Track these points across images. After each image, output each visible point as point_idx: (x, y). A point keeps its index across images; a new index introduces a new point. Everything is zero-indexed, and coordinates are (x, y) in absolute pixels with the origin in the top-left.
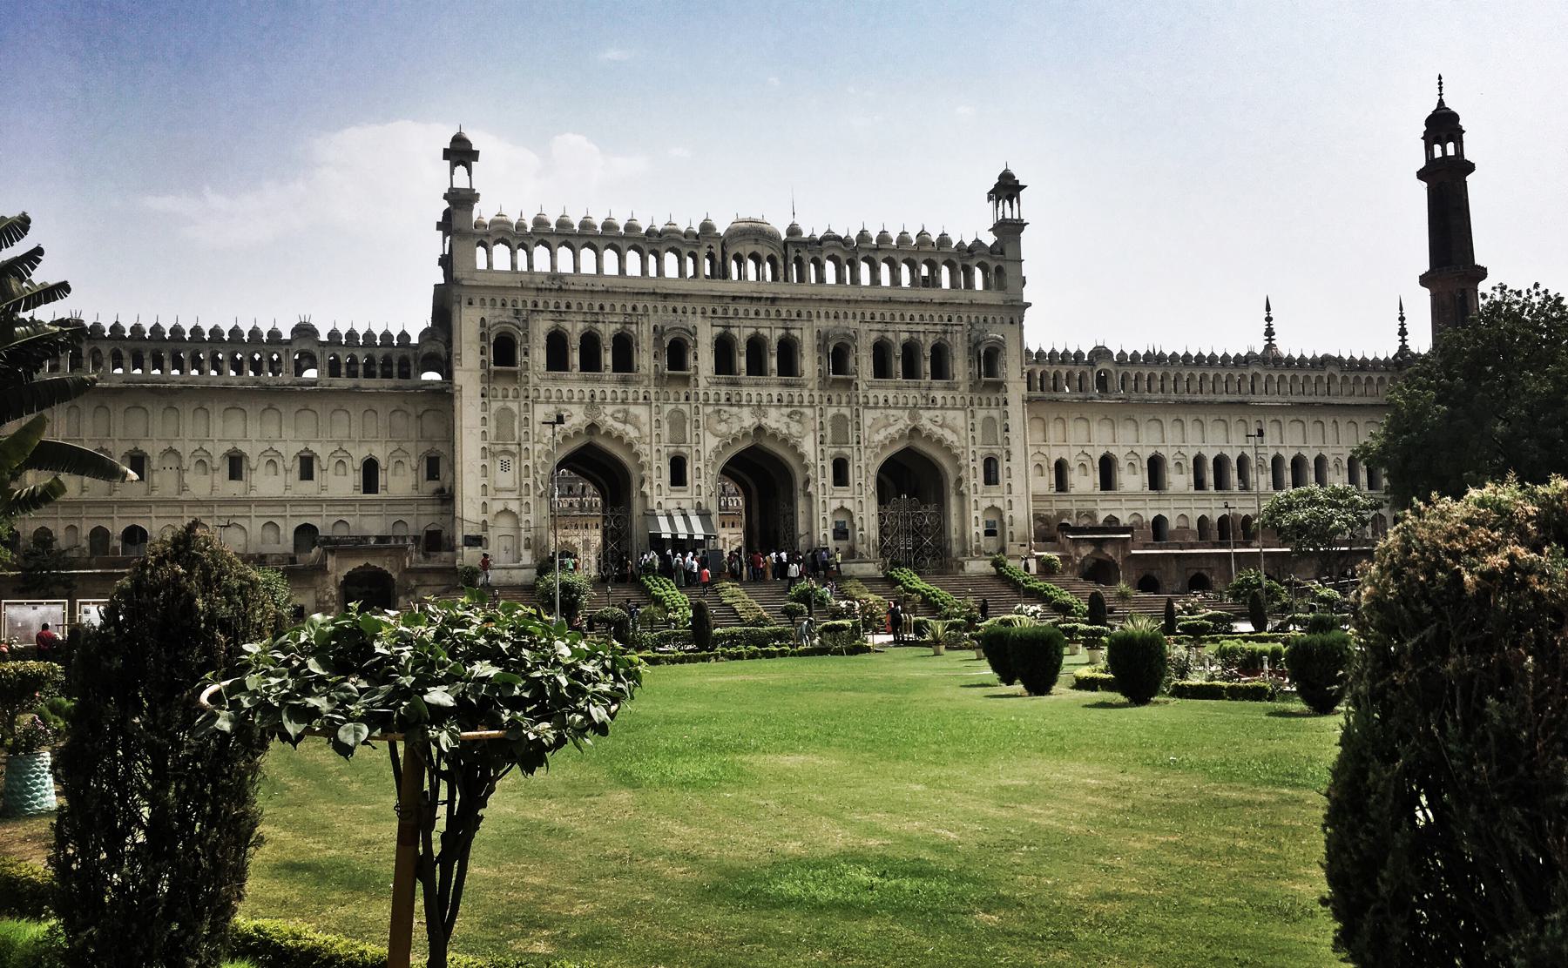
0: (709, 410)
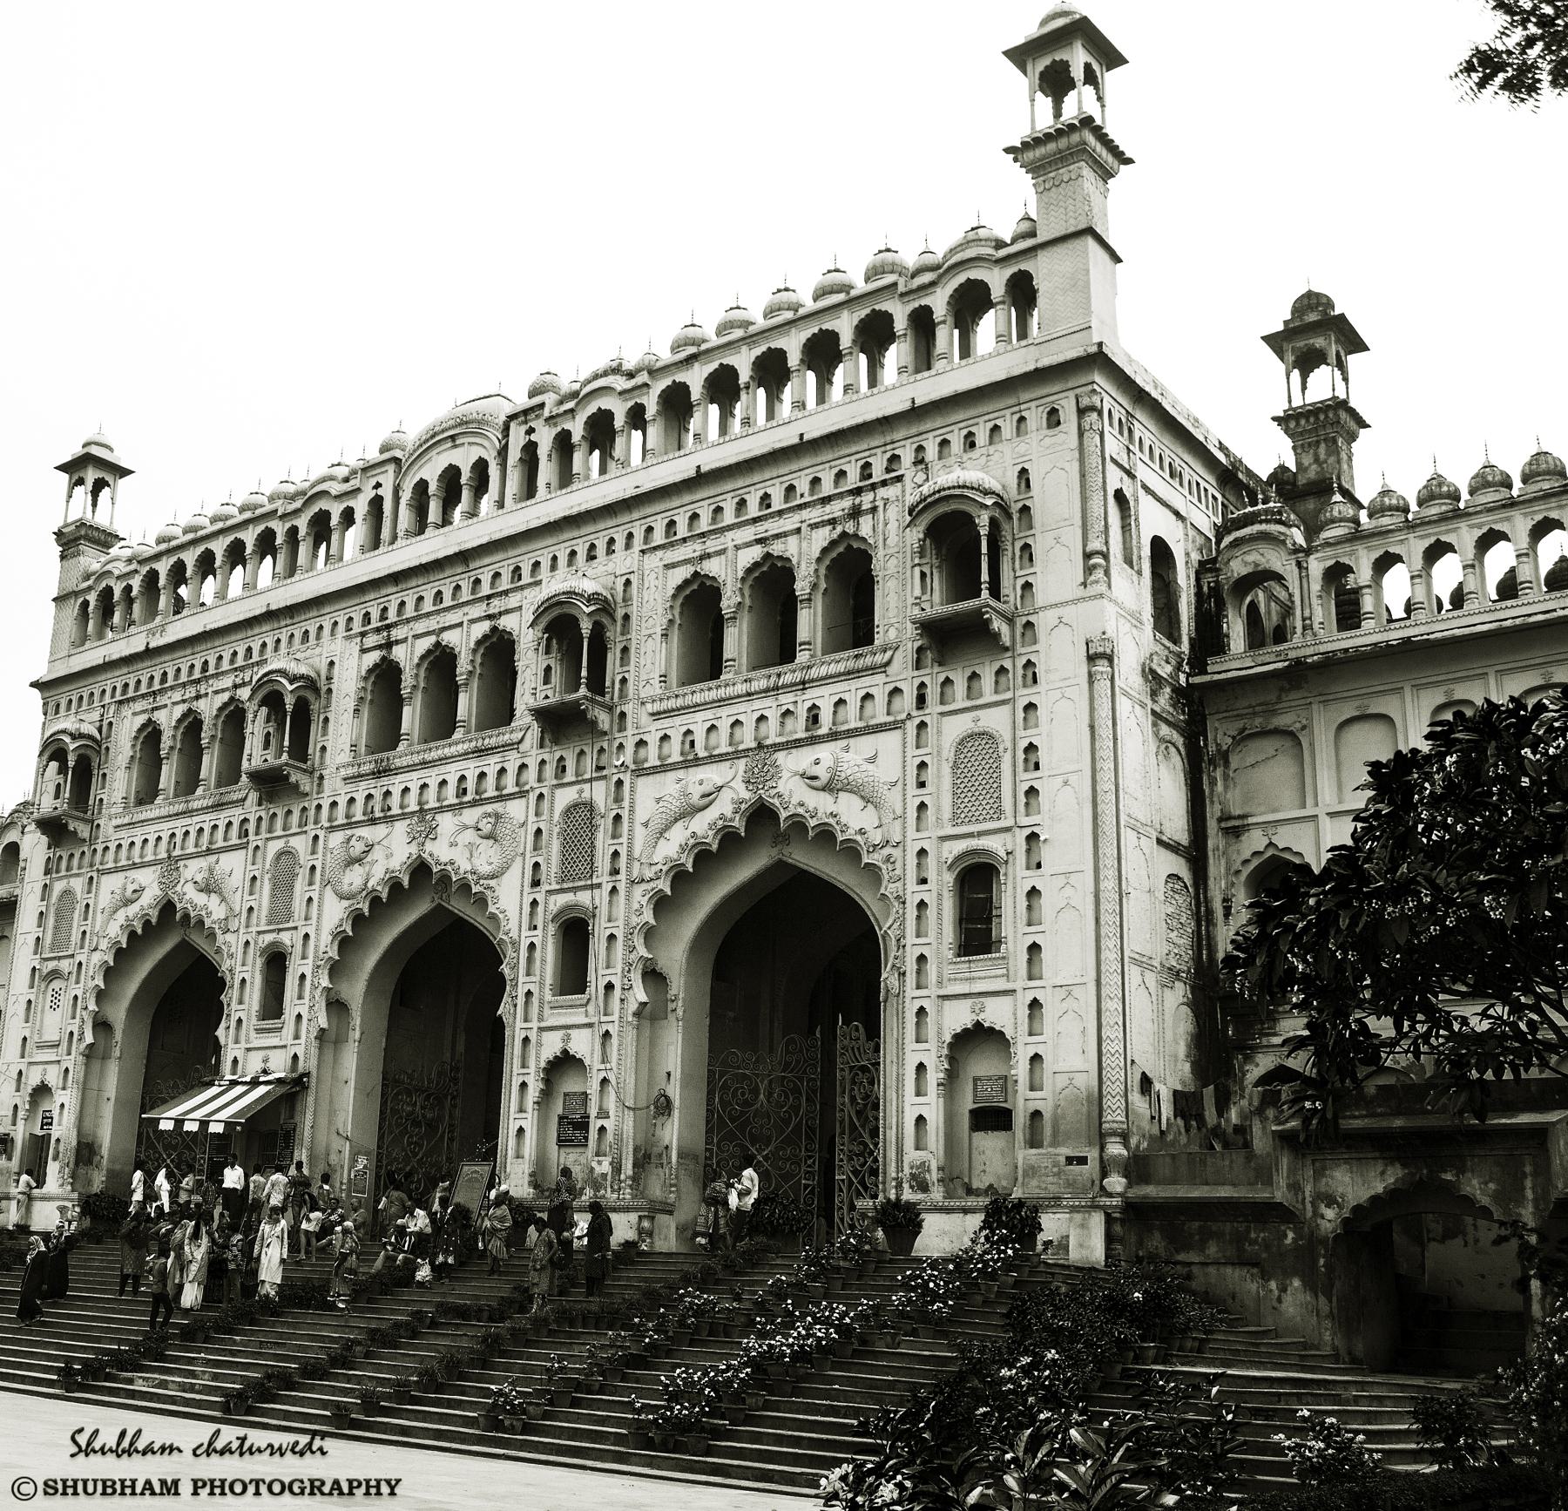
0: (337, 838)
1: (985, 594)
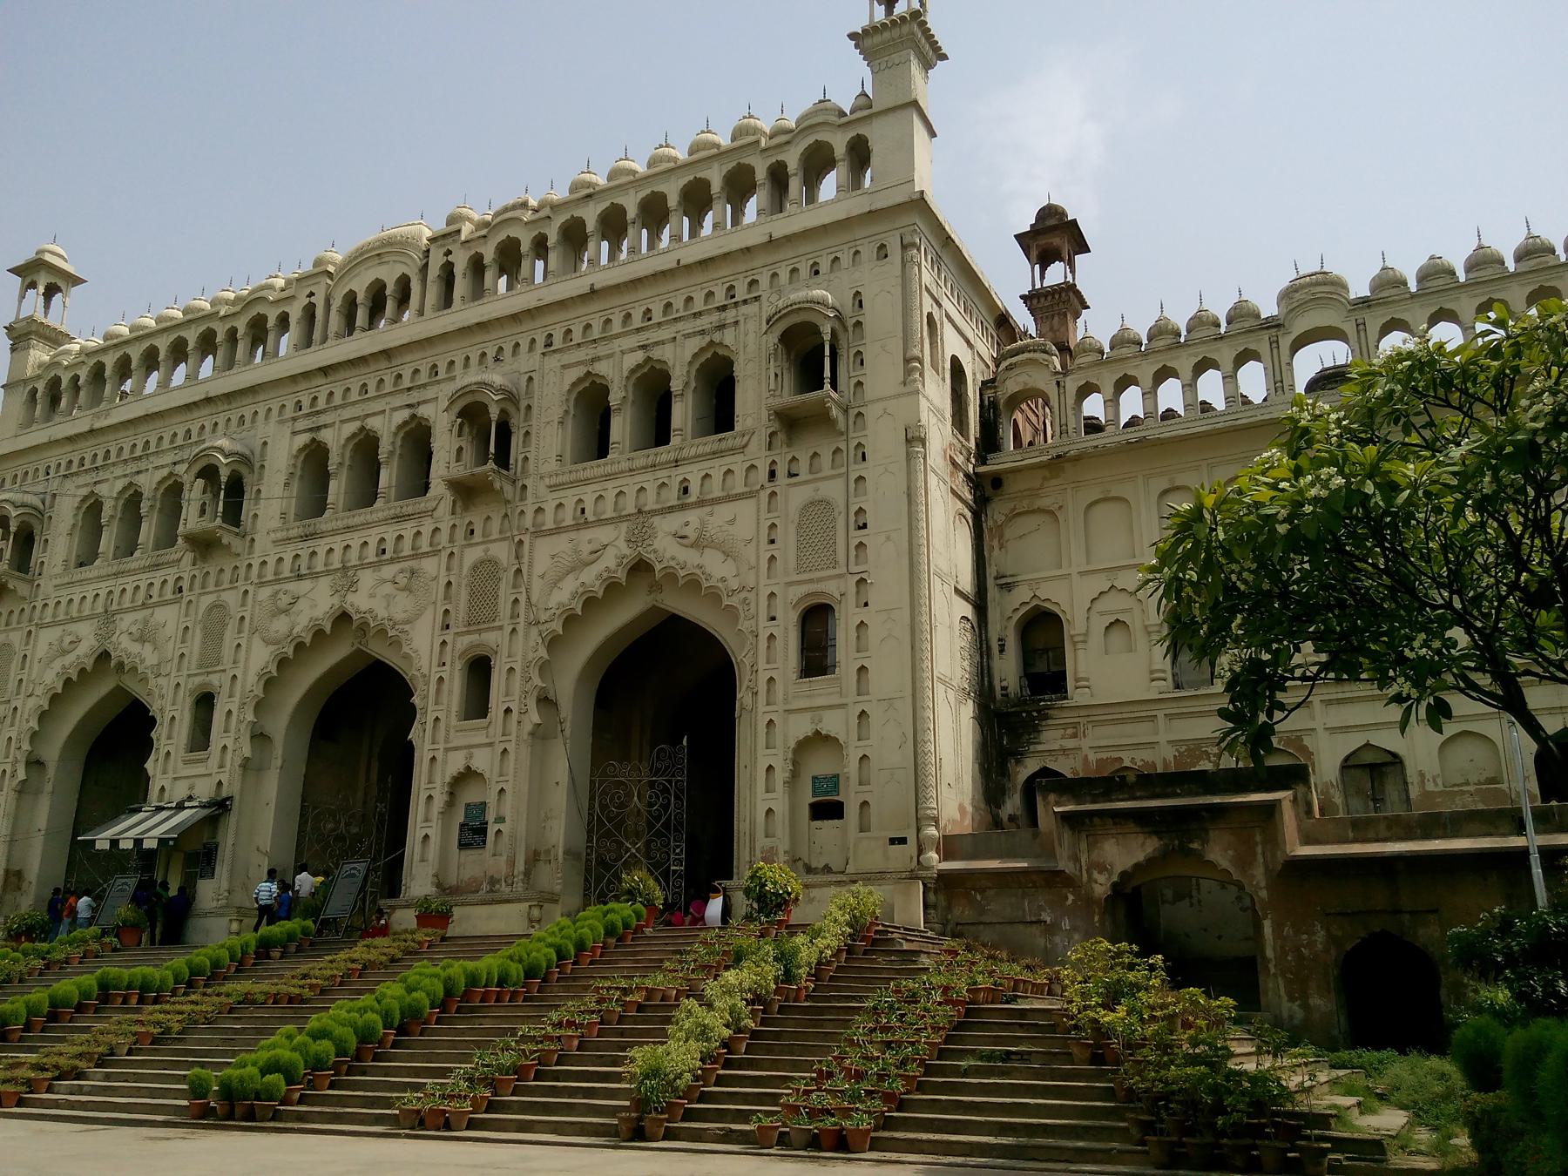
0: (265, 593)
1: (827, 386)
